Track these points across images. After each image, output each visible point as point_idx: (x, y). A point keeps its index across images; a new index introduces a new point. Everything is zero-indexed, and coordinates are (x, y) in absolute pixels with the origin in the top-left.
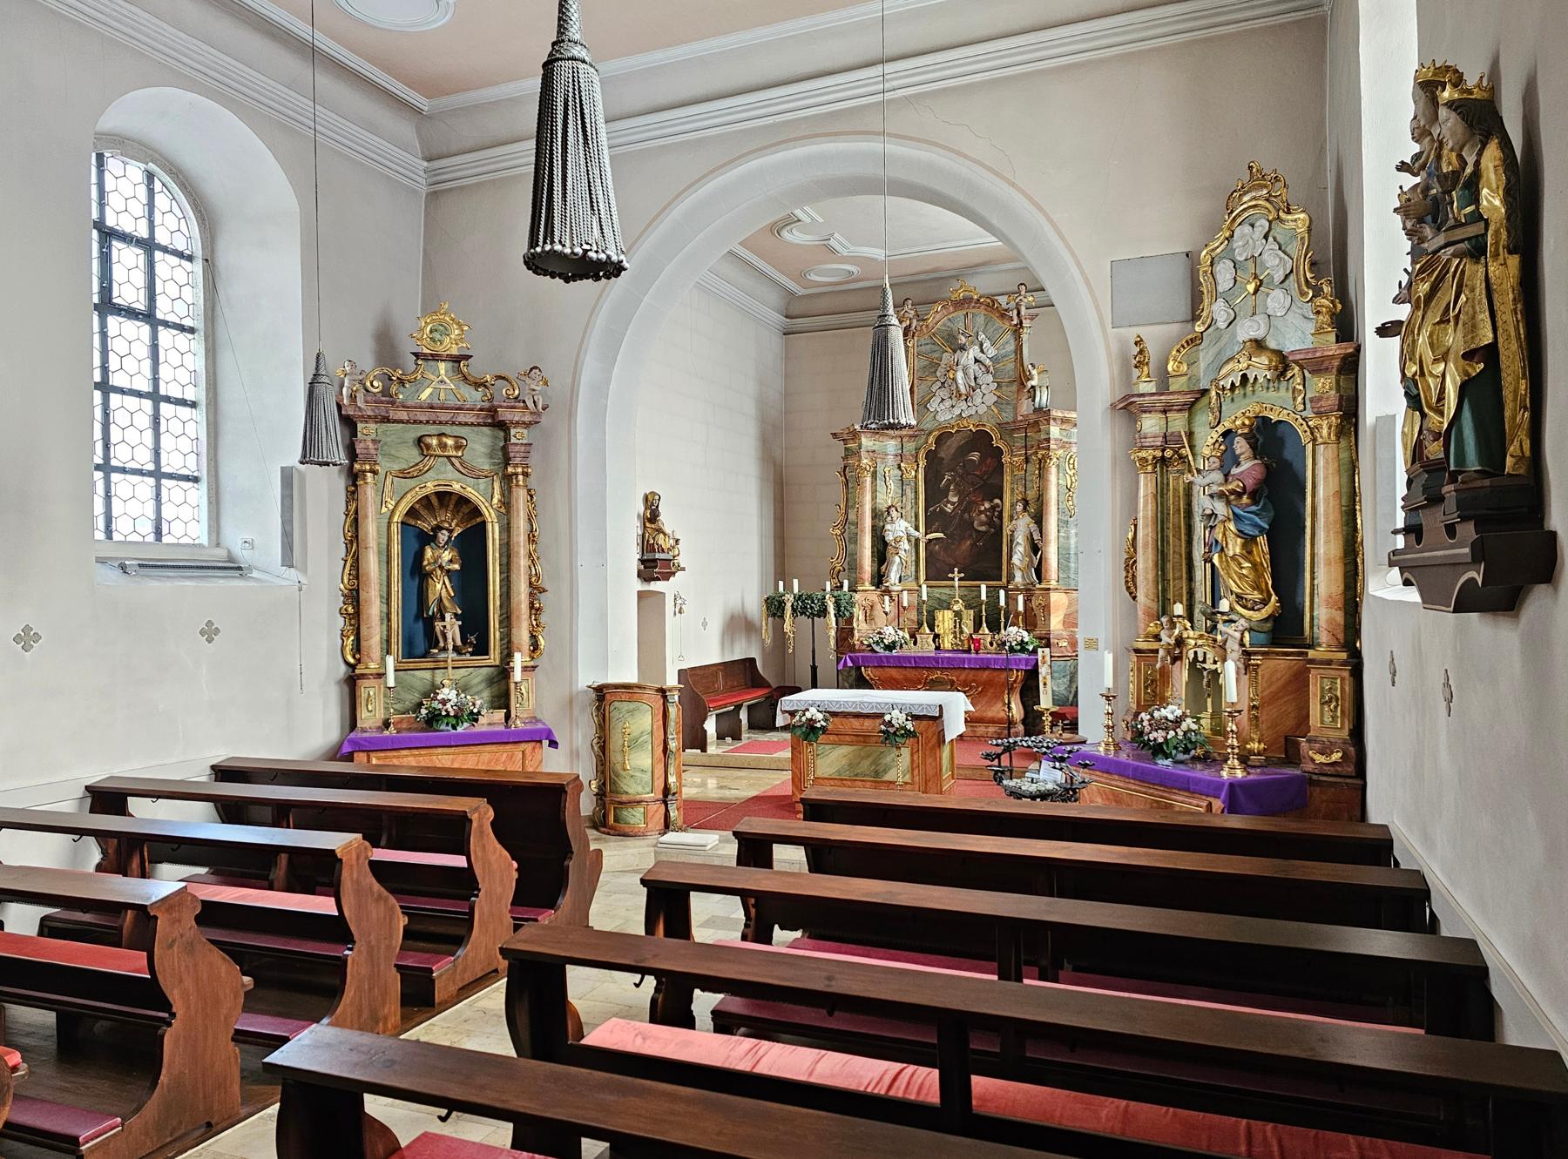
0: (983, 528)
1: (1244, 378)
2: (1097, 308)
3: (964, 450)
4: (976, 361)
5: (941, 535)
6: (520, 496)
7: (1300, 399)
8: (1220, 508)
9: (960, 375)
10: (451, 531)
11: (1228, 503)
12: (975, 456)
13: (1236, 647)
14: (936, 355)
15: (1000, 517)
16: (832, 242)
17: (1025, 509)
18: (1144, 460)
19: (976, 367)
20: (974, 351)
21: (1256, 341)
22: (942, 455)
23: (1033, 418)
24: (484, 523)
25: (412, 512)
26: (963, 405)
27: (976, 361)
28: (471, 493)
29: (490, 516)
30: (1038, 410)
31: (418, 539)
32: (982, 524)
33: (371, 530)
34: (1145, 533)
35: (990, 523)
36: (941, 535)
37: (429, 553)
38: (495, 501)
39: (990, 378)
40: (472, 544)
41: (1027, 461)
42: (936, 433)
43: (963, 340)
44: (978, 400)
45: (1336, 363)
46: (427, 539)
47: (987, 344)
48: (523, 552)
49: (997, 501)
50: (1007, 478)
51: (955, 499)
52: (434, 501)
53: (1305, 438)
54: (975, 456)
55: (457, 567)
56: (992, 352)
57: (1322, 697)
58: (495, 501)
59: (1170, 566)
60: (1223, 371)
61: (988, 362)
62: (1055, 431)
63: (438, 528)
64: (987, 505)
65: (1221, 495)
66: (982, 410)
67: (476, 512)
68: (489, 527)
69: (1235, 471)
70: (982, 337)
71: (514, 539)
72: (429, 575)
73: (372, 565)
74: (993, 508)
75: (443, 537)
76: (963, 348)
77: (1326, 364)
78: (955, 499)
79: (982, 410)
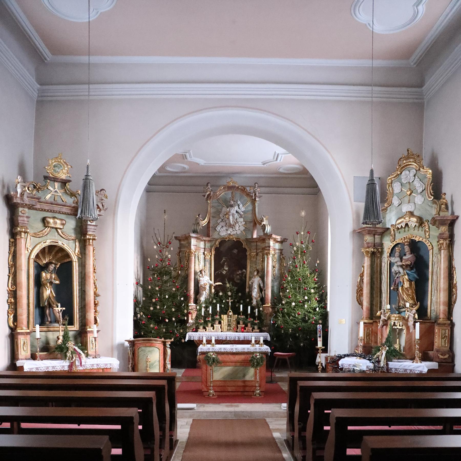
0: (238, 281)
1: (407, 225)
2: (349, 193)
3: (231, 249)
4: (237, 212)
5: (220, 283)
6: (90, 249)
7: (428, 234)
8: (401, 270)
9: (231, 217)
10: (56, 264)
11: (404, 269)
12: (235, 251)
13: (412, 319)
14: (220, 208)
15: (245, 277)
16: (188, 155)
17: (257, 274)
18: (368, 252)
19: (236, 215)
20: (236, 208)
21: (411, 212)
22: (222, 249)
23: (264, 237)
24: (71, 263)
25: (37, 256)
26: (231, 230)
27: (237, 212)
28: (66, 247)
29: (75, 259)
30: (266, 234)
31: (40, 269)
32: (238, 279)
33: (23, 261)
34: (366, 279)
35: (241, 279)
36: (220, 283)
37: (44, 274)
38: (77, 251)
39: (242, 220)
40: (65, 271)
41: (257, 255)
42: (219, 240)
43: (232, 202)
44: (237, 228)
45: (449, 222)
46: (45, 268)
47: (241, 206)
48: (92, 276)
49: (244, 270)
50: (248, 261)
51: (227, 269)
52: (47, 250)
53: (430, 248)
54: (235, 251)
55: (57, 282)
56: (243, 209)
57: (442, 336)
58: (77, 251)
59: (374, 292)
60: (398, 222)
61: (242, 213)
62: (272, 243)
63: (50, 263)
64: (240, 272)
65: (402, 266)
66: (239, 232)
67: (68, 255)
68: (74, 263)
69: (404, 257)
70: (239, 202)
71: (87, 270)
72: (44, 285)
73: (23, 278)
74: (242, 273)
75: (52, 267)
76: (232, 206)
77: (446, 222)
78: (227, 269)
79: (239, 232)
